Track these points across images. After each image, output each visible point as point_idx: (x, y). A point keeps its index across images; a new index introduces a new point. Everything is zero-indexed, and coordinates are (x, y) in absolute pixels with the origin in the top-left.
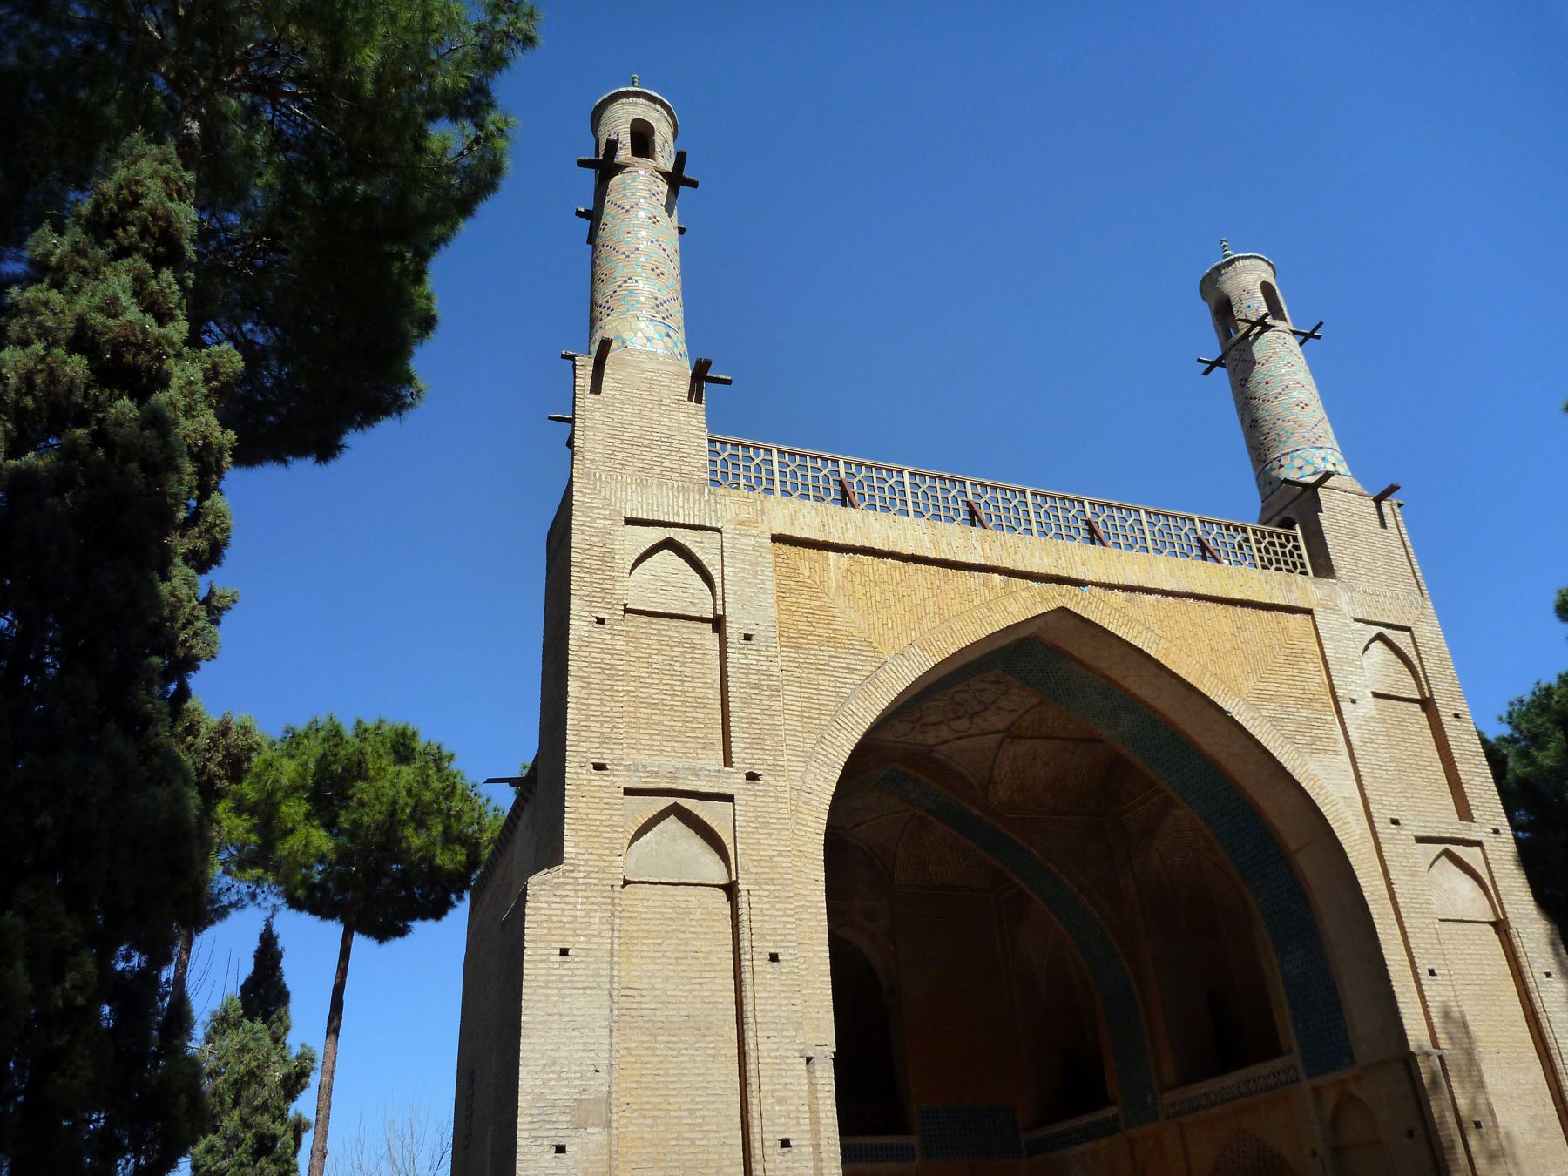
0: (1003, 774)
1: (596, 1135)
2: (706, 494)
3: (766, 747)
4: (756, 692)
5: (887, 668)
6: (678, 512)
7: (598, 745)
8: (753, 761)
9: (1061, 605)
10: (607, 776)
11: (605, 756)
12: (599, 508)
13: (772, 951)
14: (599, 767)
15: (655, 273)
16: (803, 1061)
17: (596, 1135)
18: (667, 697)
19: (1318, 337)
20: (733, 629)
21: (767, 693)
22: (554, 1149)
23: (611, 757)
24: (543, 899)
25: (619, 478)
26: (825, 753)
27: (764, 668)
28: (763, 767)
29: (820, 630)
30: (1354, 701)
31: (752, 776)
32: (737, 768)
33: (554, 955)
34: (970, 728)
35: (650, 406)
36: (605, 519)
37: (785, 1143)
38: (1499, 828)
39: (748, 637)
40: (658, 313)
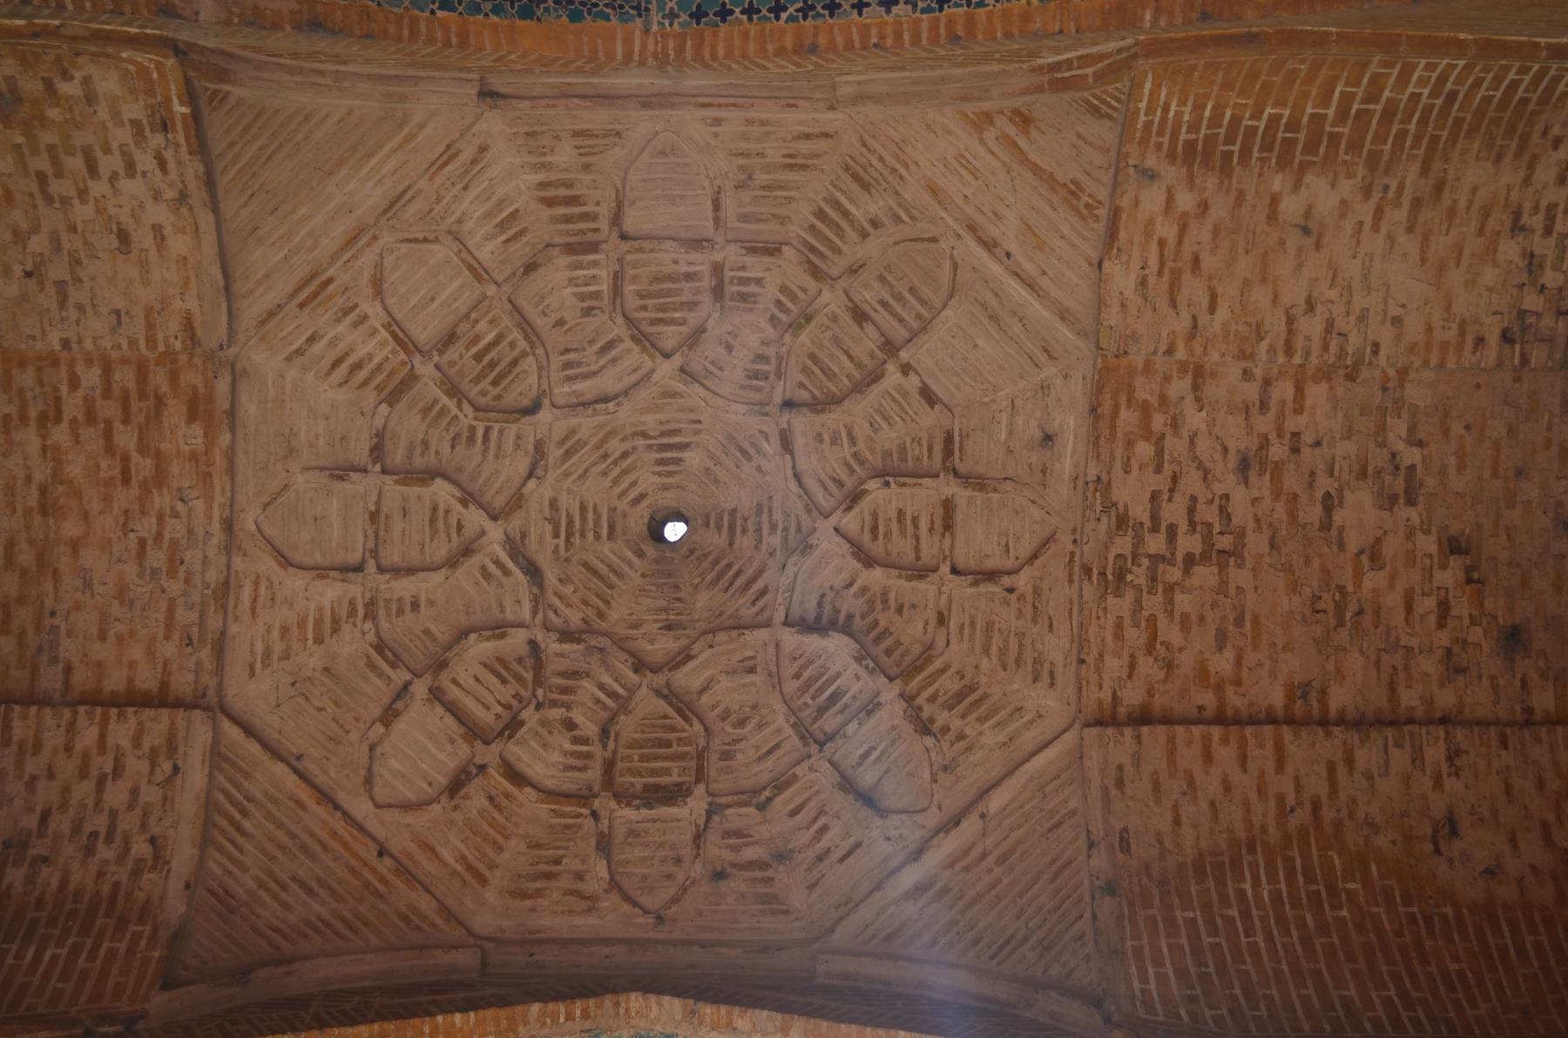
0: (145, 161)
34: (378, 285)
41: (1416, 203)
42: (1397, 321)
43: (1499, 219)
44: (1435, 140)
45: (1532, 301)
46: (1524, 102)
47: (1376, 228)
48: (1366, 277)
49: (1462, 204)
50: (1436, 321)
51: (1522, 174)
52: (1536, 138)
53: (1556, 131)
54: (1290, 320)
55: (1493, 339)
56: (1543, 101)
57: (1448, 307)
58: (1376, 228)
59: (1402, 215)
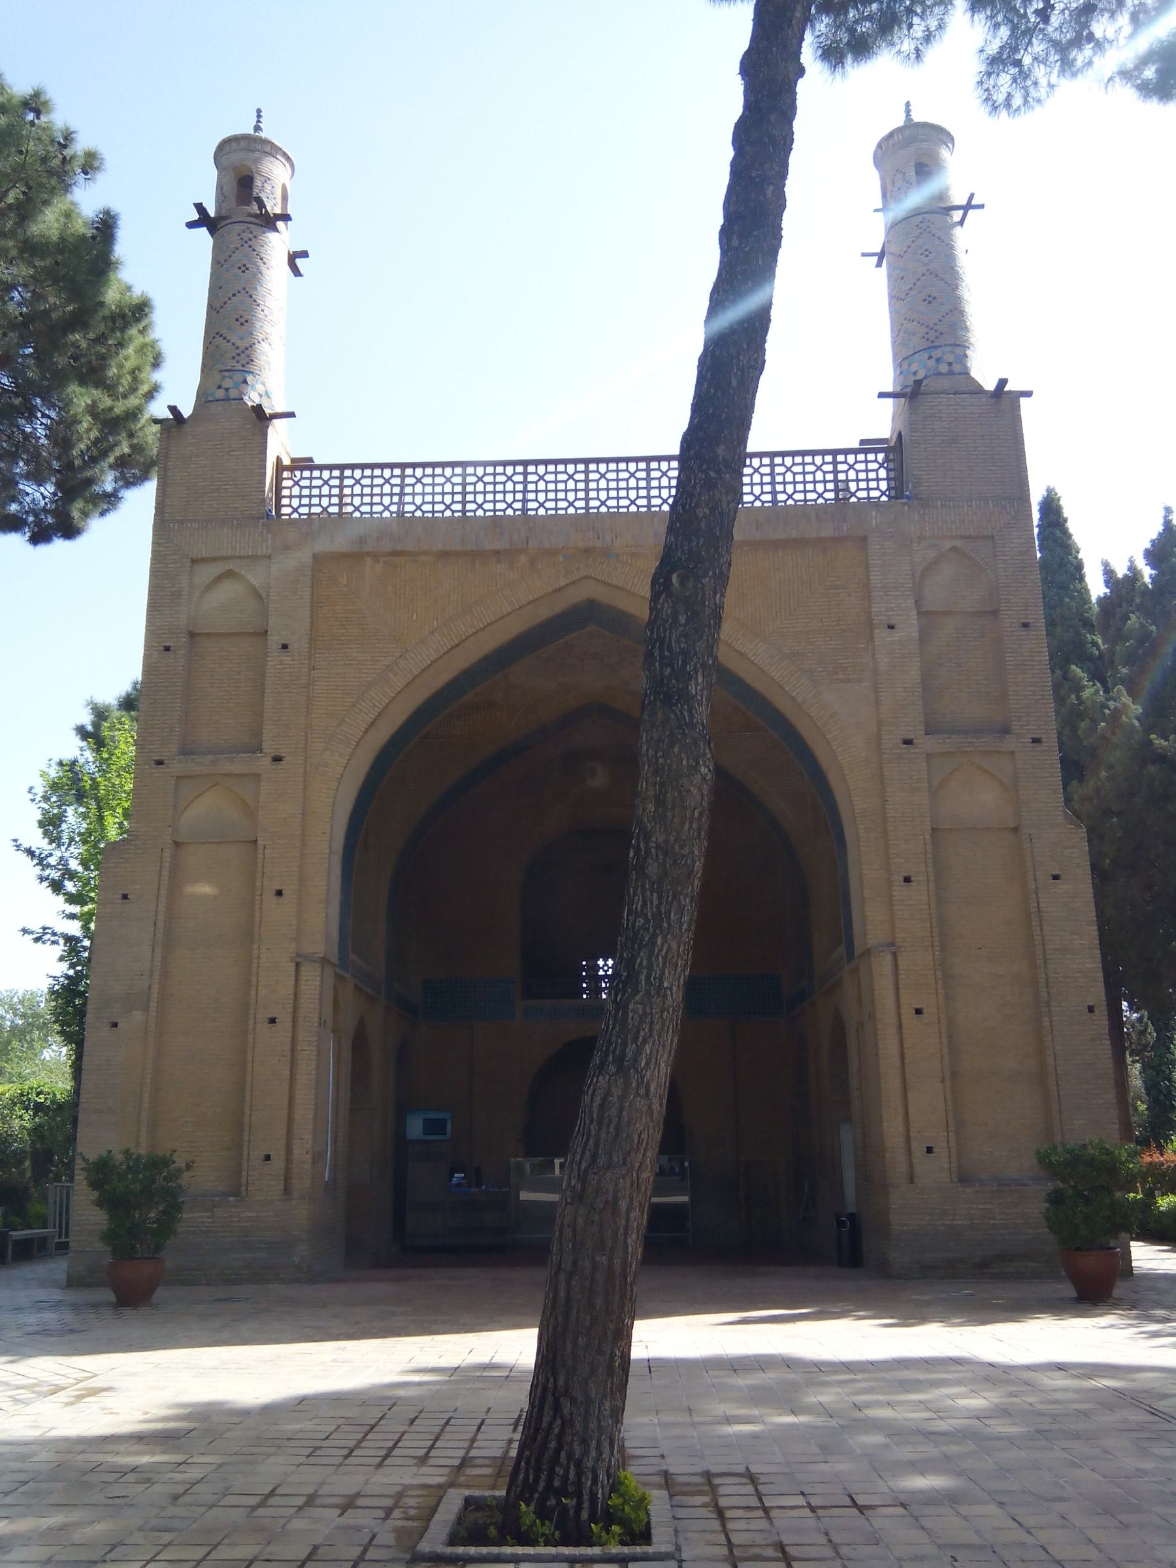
1: (138, 1015)
2: (260, 527)
3: (290, 735)
4: (287, 690)
5: (408, 657)
6: (236, 546)
7: (158, 746)
8: (279, 747)
9: (585, 574)
10: (164, 769)
11: (164, 754)
12: (171, 554)
13: (278, 888)
14: (160, 763)
15: (239, 323)
16: (293, 965)
17: (138, 1015)
18: (225, 701)
19: (981, 206)
20: (274, 640)
22: (110, 1025)
23: (168, 754)
24: (112, 861)
25: (189, 525)
26: (343, 733)
27: (296, 670)
28: (286, 750)
29: (351, 631)
30: (891, 627)
31: (277, 759)
32: (266, 753)
33: (117, 899)
35: (220, 454)
36: (176, 563)
37: (273, 1021)
38: (1042, 736)
39: (285, 647)
40: (238, 362)
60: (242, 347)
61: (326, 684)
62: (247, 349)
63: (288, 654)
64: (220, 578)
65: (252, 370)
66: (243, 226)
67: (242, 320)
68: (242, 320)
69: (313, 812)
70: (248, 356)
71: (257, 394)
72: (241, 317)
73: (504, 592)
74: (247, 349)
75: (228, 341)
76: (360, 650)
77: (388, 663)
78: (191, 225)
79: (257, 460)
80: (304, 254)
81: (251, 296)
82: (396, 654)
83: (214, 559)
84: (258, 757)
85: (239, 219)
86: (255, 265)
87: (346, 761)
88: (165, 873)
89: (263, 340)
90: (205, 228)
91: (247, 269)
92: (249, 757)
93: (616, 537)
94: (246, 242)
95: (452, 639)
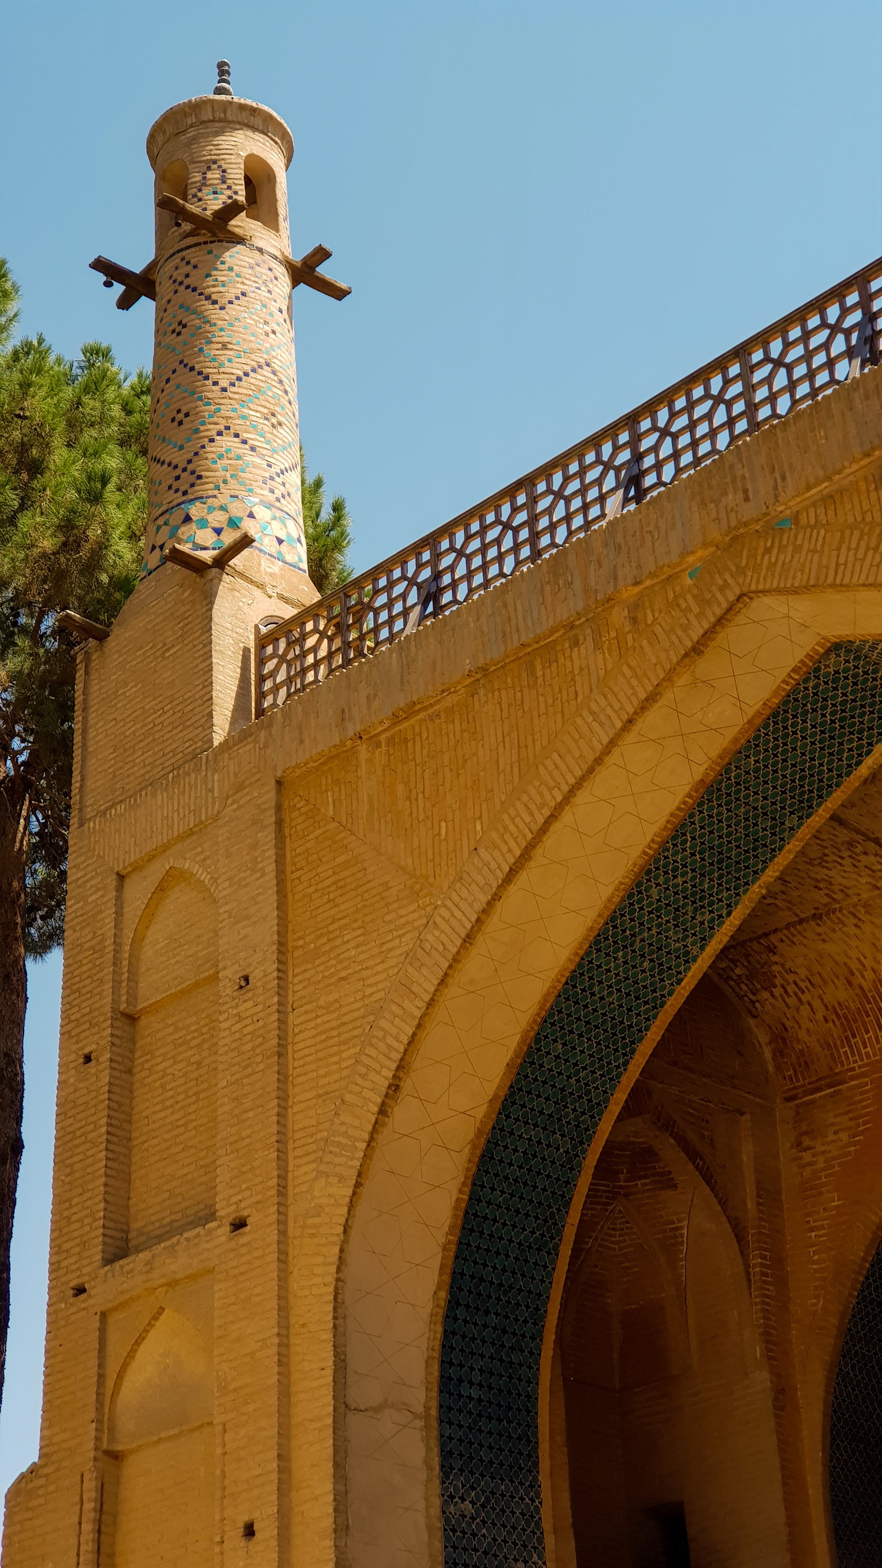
9: (738, 592)
21: (261, 1067)
32: (222, 1218)
41: (852, 974)
42: (820, 934)
43: (816, 980)
44: (869, 1003)
45: (774, 958)
46: (854, 1036)
47: (858, 959)
48: (846, 943)
49: (836, 980)
50: (805, 941)
51: (825, 1000)
52: (834, 1017)
53: (831, 1024)
54: (860, 920)
55: (777, 944)
56: (847, 1038)
57: (805, 946)
58: (858, 959)
59: (853, 968)
60: (181, 466)
61: (314, 1032)
62: (190, 462)
63: (250, 995)
64: (161, 889)
65: (199, 494)
66: (176, 260)
67: (181, 416)
68: (181, 416)
69: (303, 1325)
70: (193, 472)
71: (210, 530)
72: (179, 411)
73: (593, 705)
74: (190, 462)
75: (163, 463)
76: (362, 939)
77: (405, 949)
78: (125, 303)
79: (201, 646)
80: (321, 254)
81: (192, 369)
82: (417, 924)
83: (151, 858)
84: (210, 1232)
85: (171, 251)
86: (195, 312)
87: (350, 1192)
88: (87, 1527)
89: (220, 433)
90: (143, 297)
91: (185, 326)
92: (198, 1235)
93: (784, 478)
94: (181, 283)
95: (510, 851)
